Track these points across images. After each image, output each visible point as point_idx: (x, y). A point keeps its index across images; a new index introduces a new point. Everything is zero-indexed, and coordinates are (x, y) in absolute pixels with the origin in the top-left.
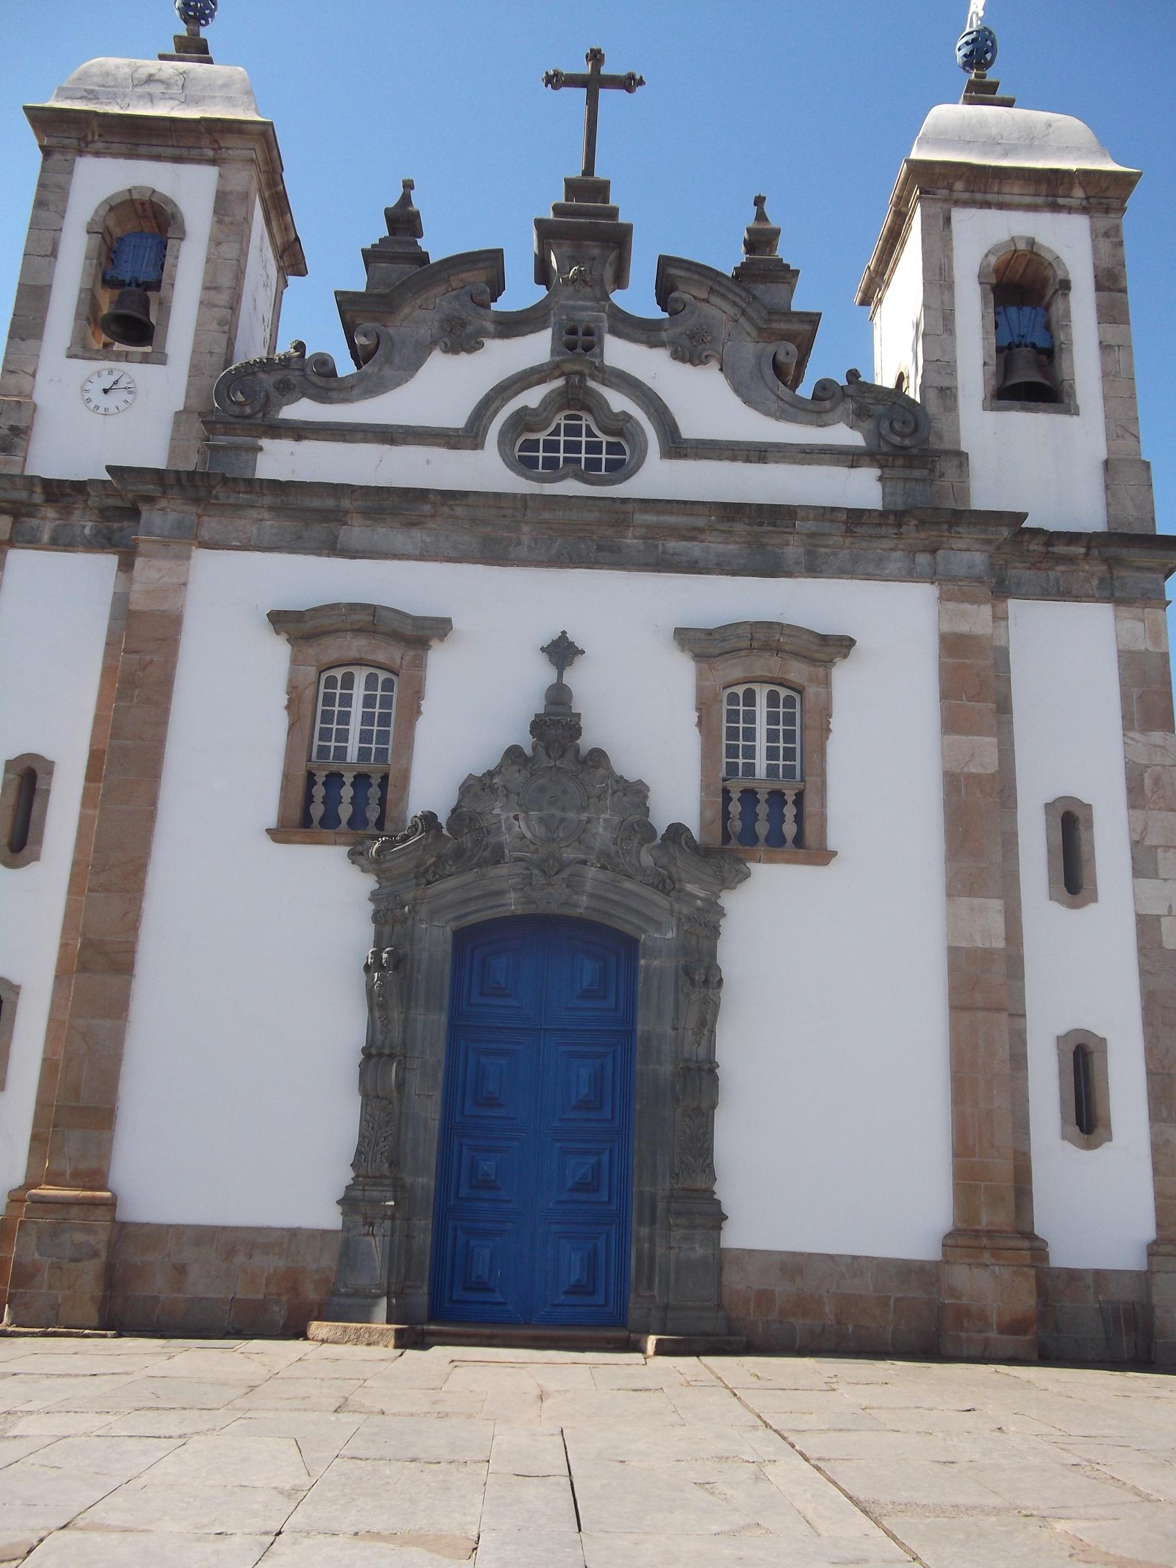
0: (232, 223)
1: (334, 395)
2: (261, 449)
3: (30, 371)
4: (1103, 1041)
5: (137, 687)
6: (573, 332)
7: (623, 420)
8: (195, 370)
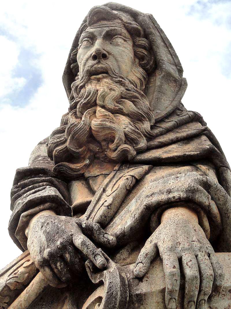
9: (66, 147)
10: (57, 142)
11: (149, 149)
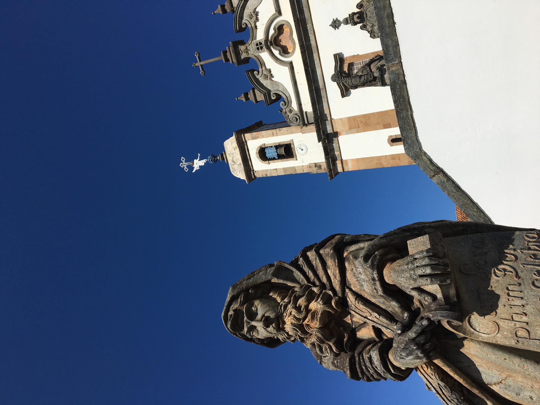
0: (258, 135)
1: (289, 99)
2: (306, 112)
3: (302, 167)
5: (367, 122)
6: (258, 49)
7: (275, 29)
8: (292, 133)
9: (333, 344)
10: (330, 350)
11: (333, 289)
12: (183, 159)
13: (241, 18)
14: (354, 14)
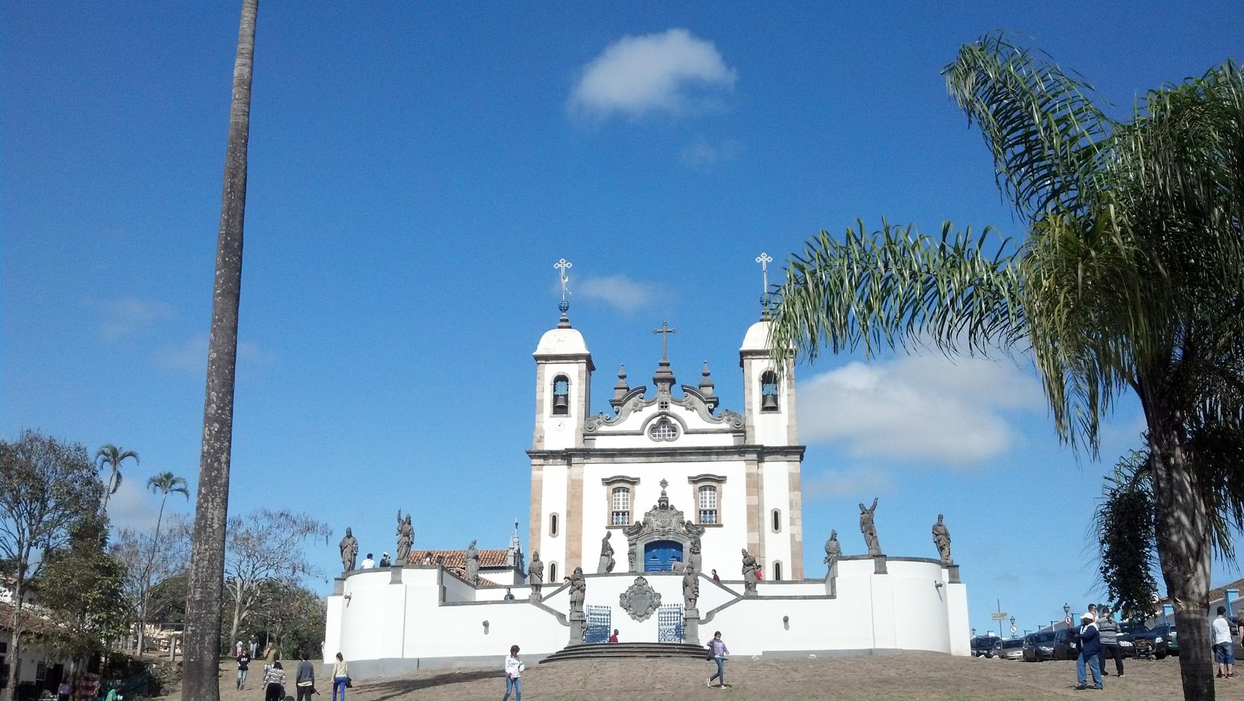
2: (595, 439)
4: (782, 562)
6: (662, 403)
8: (578, 418)
12: (569, 265)
13: (692, 393)
14: (667, 503)
